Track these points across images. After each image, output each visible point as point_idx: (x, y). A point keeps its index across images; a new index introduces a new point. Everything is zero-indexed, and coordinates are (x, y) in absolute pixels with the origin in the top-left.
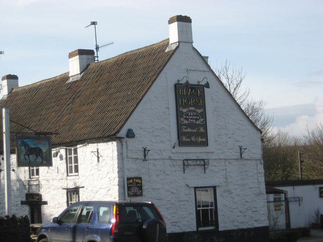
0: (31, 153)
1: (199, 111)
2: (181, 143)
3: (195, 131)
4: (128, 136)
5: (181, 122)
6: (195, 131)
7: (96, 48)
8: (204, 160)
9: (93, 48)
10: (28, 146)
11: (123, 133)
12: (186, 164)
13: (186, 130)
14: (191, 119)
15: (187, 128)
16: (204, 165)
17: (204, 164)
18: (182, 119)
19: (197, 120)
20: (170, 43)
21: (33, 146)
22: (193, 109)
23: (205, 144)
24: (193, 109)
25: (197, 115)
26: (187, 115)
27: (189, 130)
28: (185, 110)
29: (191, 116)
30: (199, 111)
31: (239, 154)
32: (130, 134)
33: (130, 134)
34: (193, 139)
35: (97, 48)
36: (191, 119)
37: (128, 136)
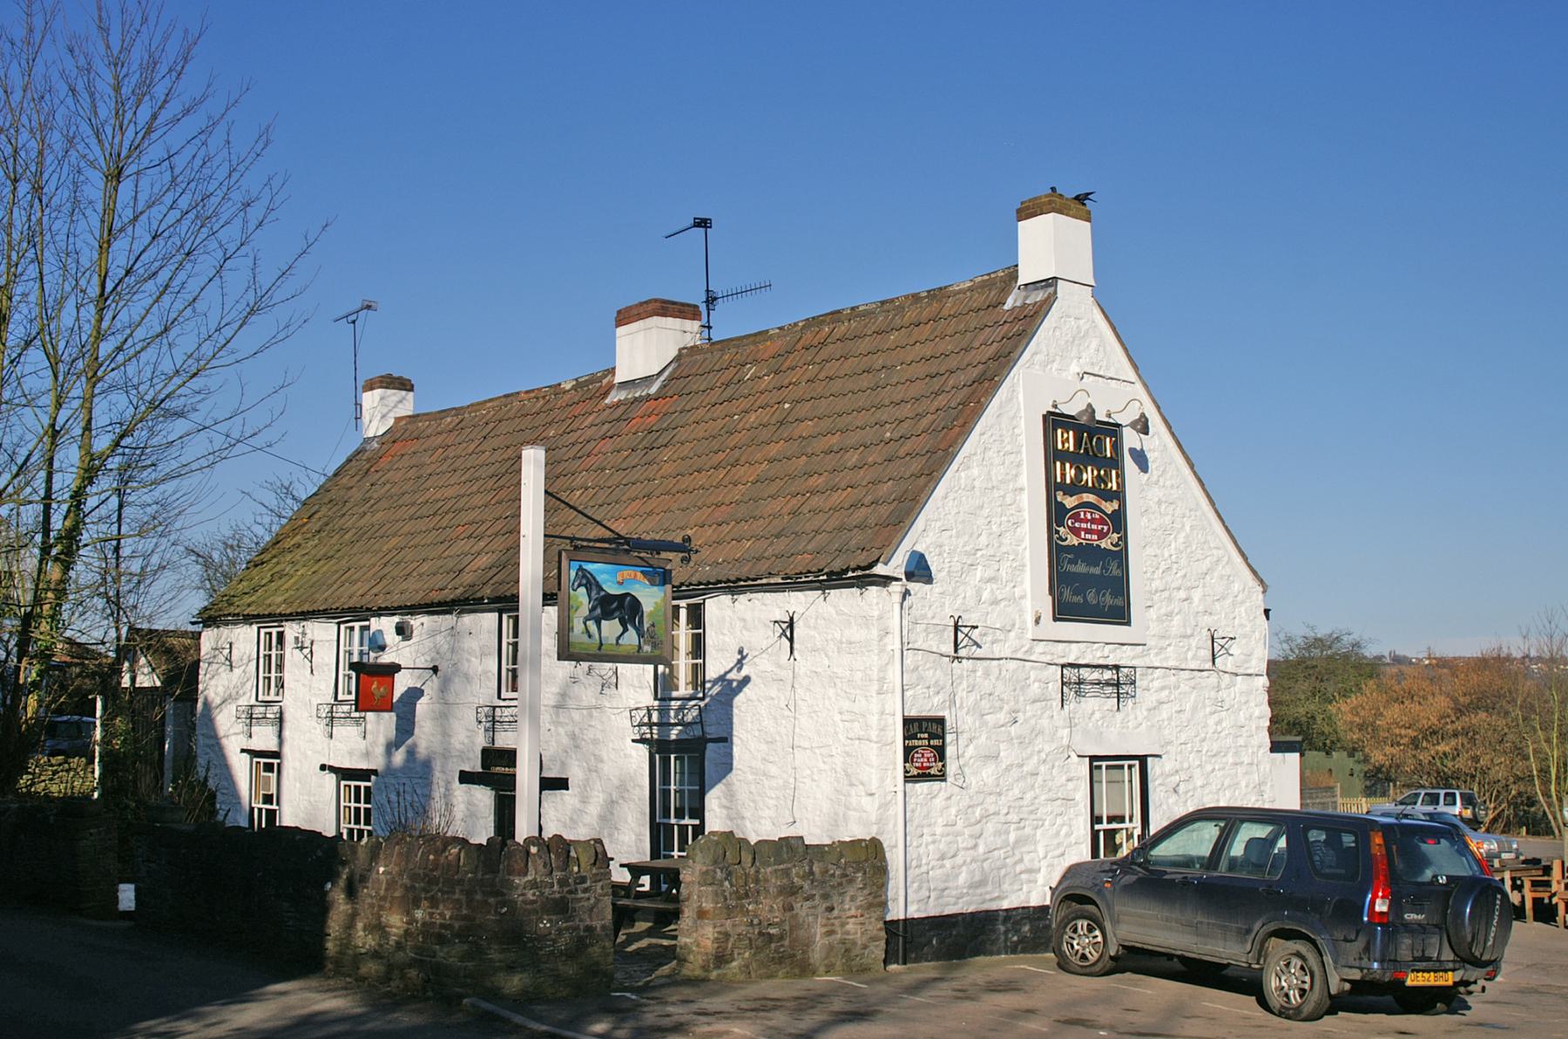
0: (607, 615)
1: (1110, 507)
2: (1063, 612)
3: (1096, 571)
4: (910, 576)
5: (1060, 538)
6: (1096, 571)
7: (707, 302)
8: (1117, 667)
9: (698, 299)
10: (600, 589)
11: (895, 565)
12: (1074, 681)
13: (1073, 568)
14: (1087, 531)
15: (1073, 562)
16: (1118, 685)
17: (1119, 683)
18: (1061, 529)
19: (1102, 535)
20: (1021, 281)
21: (613, 589)
22: (1090, 498)
23: (1119, 615)
24: (1090, 498)
25: (1101, 521)
26: (1076, 517)
27: (1081, 568)
28: (1070, 502)
29: (1086, 521)
30: (1110, 507)
31: (1208, 654)
32: (919, 570)
33: (919, 570)
34: (1091, 597)
35: (711, 300)
36: (1087, 531)
37: (910, 576)
